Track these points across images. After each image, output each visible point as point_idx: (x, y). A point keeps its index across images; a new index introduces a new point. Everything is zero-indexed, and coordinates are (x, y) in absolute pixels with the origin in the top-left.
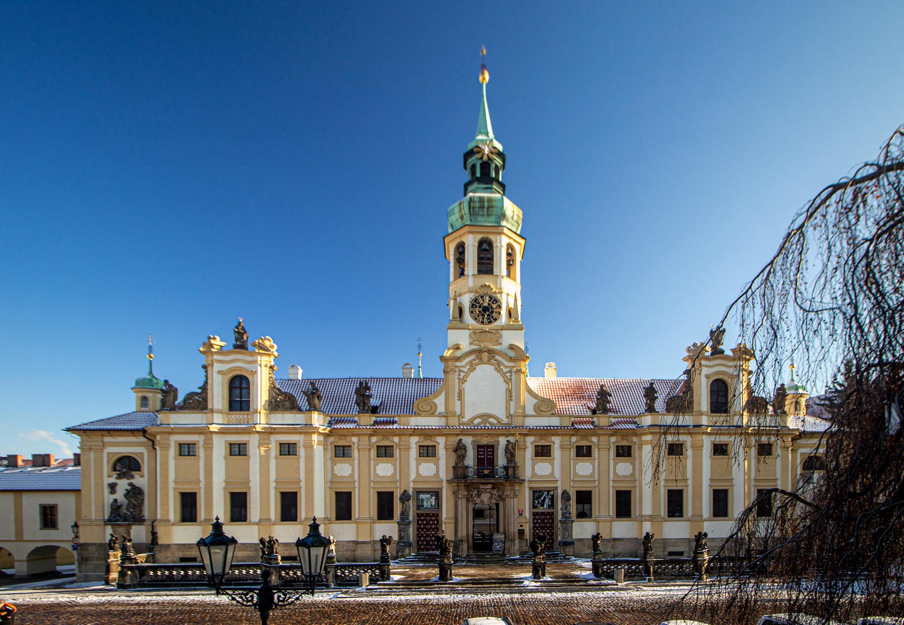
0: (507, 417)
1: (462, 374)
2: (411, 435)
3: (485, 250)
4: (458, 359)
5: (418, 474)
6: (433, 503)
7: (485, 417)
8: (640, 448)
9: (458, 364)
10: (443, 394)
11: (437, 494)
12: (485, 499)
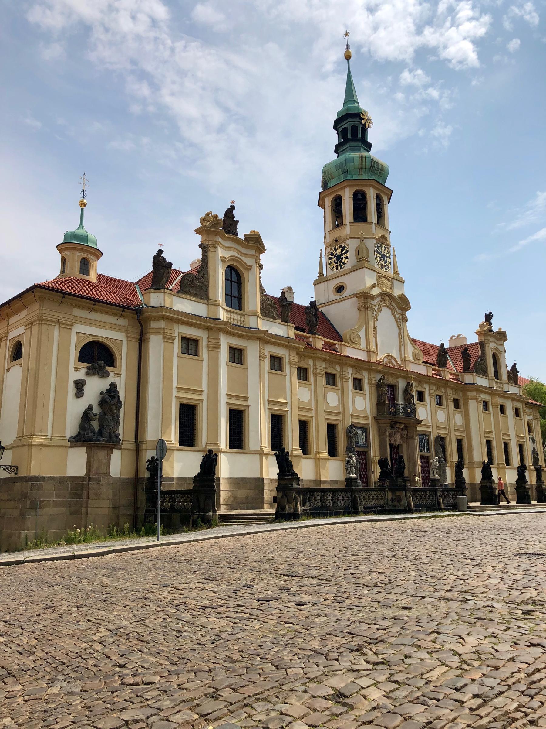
0: (402, 360)
1: (375, 313)
2: (350, 366)
3: (359, 200)
4: (373, 298)
5: (354, 407)
6: (364, 440)
7: (390, 357)
8: (466, 403)
9: (373, 302)
10: (364, 328)
11: (365, 429)
12: (398, 439)
